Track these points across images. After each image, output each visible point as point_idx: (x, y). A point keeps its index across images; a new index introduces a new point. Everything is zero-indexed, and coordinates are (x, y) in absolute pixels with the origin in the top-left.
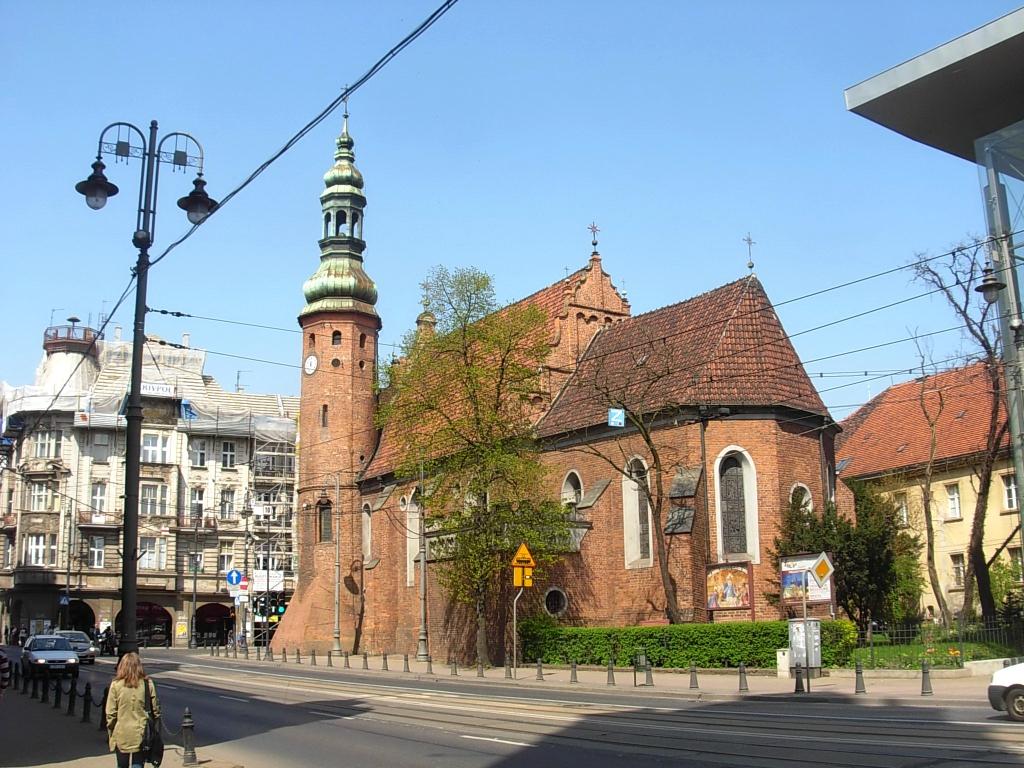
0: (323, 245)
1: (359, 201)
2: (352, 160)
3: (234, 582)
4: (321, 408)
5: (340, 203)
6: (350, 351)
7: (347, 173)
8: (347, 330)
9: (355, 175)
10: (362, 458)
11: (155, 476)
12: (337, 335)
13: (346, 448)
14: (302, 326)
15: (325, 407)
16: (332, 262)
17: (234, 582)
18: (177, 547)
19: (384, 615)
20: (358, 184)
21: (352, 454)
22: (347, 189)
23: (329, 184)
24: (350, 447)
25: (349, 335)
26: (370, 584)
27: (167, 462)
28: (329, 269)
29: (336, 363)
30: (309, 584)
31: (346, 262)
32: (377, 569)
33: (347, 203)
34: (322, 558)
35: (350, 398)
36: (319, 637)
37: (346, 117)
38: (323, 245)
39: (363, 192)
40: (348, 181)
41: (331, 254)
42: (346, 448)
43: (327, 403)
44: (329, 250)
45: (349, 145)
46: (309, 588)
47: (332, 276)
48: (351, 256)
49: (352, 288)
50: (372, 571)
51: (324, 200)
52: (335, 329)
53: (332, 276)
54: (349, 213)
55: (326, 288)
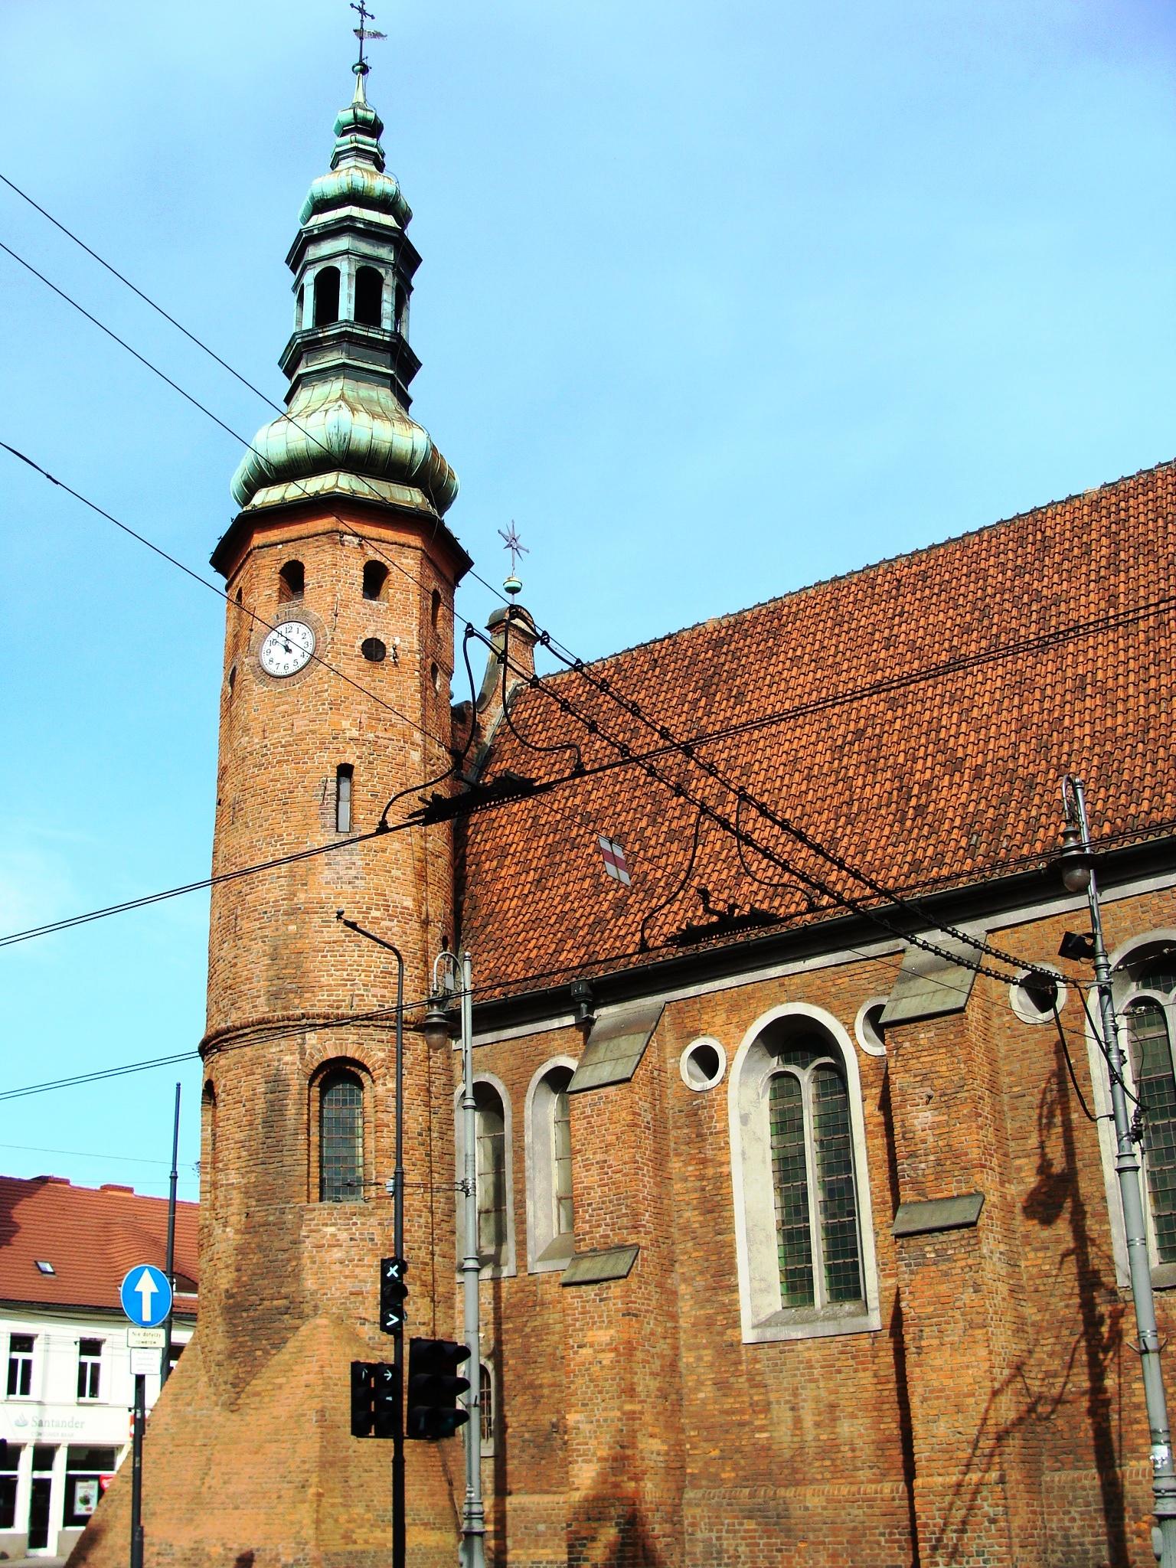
3: (147, 1316)
4: (333, 775)
5: (365, 248)
13: (409, 903)
15: (345, 771)
17: (147, 1316)
21: (425, 923)
24: (420, 902)
26: (603, 1336)
29: (373, 650)
30: (278, 1346)
32: (633, 1282)
33: (386, 253)
34: (337, 1254)
35: (416, 756)
36: (360, 1534)
37: (365, 70)
40: (388, 203)
41: (344, 365)
43: (351, 760)
46: (284, 1356)
49: (419, 458)
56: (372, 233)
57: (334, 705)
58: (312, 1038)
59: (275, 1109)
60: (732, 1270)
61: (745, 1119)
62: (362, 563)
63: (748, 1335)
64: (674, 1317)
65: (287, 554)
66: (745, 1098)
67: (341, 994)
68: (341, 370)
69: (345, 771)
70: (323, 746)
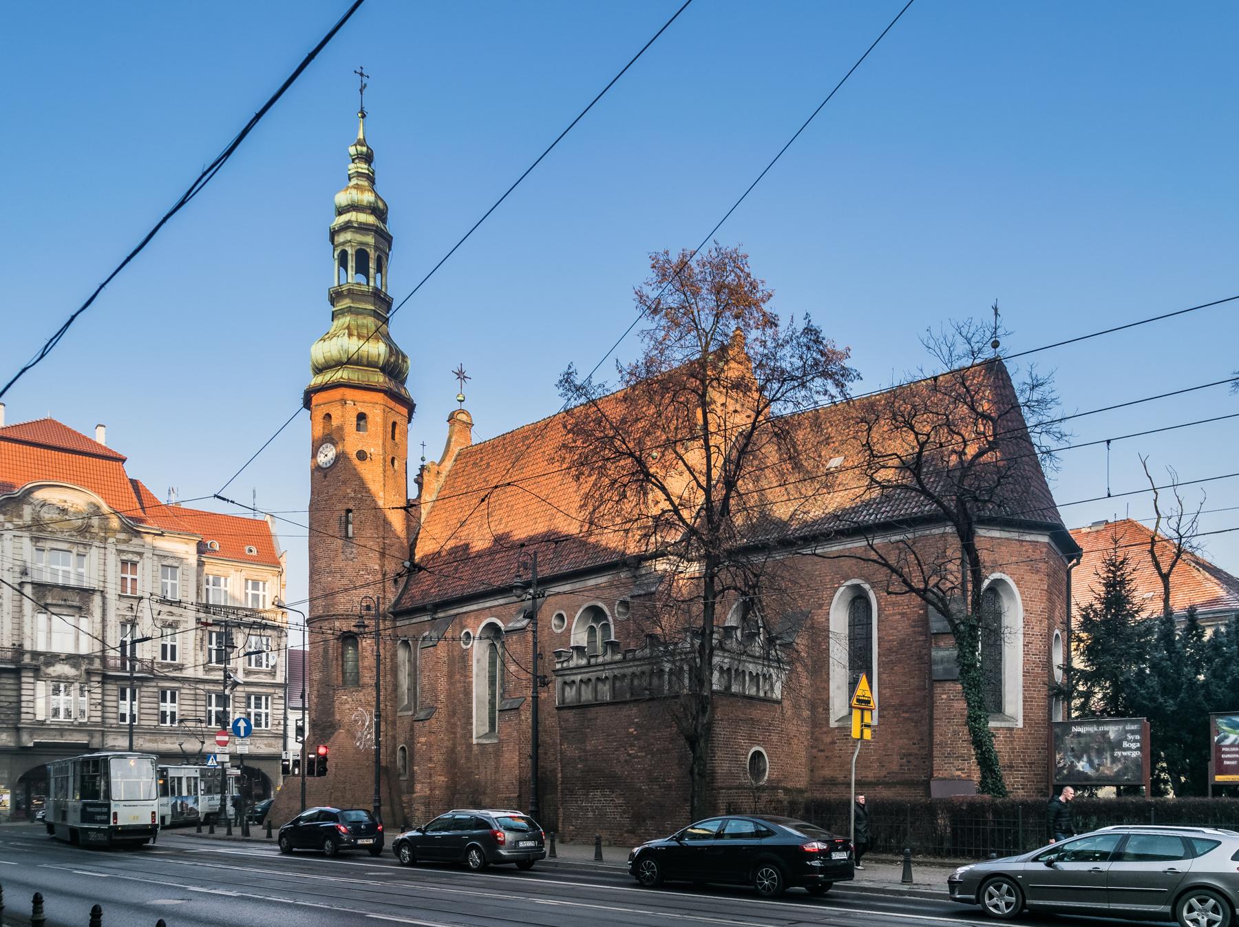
0: (335, 297)
1: (385, 239)
2: (371, 179)
5: (359, 238)
6: (380, 442)
7: (368, 197)
8: (375, 407)
9: (380, 204)
10: (396, 581)
11: (69, 603)
12: (361, 417)
13: (377, 567)
14: (307, 404)
16: (346, 320)
18: (20, 702)
19: (442, 778)
20: (380, 212)
21: (384, 575)
22: (371, 219)
23: (341, 211)
24: (382, 566)
25: (379, 419)
27: (85, 585)
28: (348, 328)
31: (370, 322)
33: (370, 239)
38: (335, 297)
39: (391, 227)
42: (377, 567)
44: (345, 303)
45: (368, 158)
47: (355, 339)
48: (376, 315)
50: (427, 723)
51: (333, 234)
52: (361, 410)
53: (355, 339)
54: (372, 254)
55: (347, 352)
56: (363, 228)
57: (344, 482)
58: (337, 624)
59: (326, 651)
60: (471, 717)
61: (478, 661)
62: (355, 414)
63: (475, 741)
64: (455, 733)
65: (324, 410)
66: (479, 652)
67: (349, 606)
68: (349, 310)
69: (349, 511)
70: (340, 501)
